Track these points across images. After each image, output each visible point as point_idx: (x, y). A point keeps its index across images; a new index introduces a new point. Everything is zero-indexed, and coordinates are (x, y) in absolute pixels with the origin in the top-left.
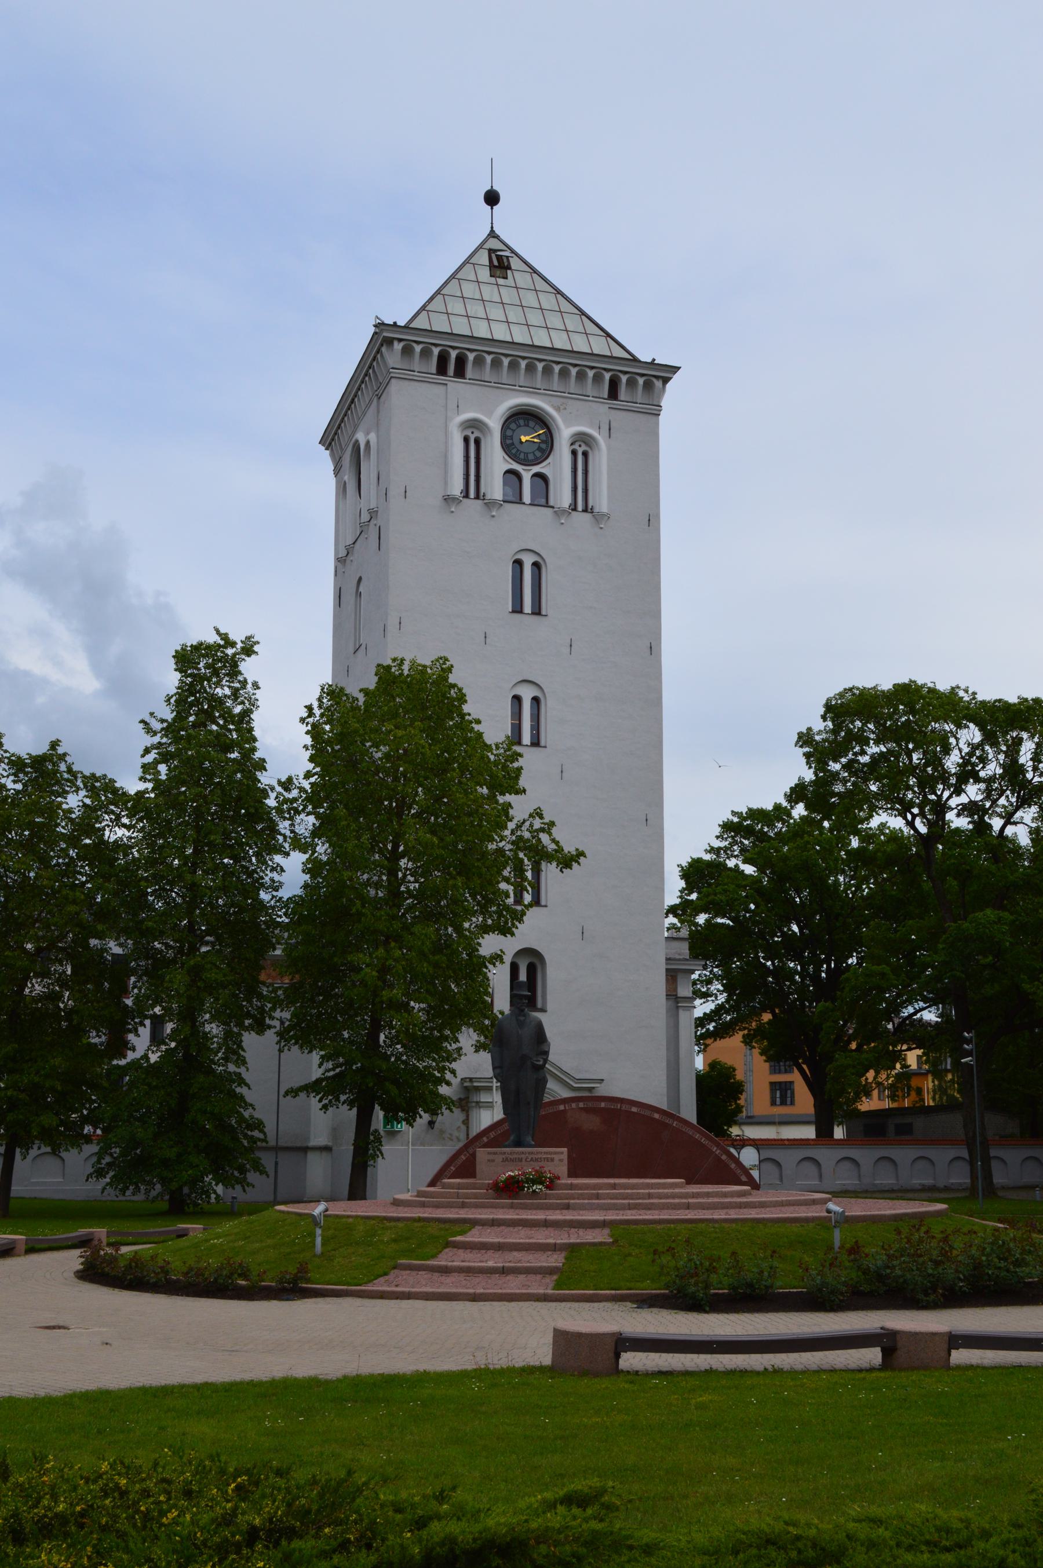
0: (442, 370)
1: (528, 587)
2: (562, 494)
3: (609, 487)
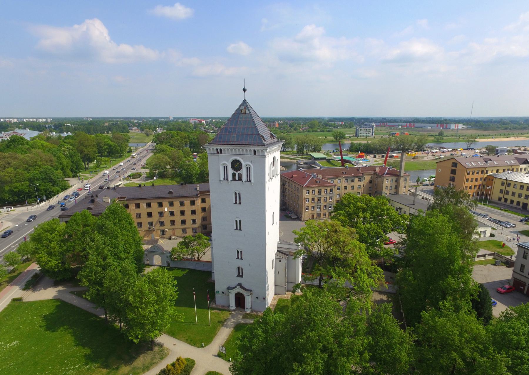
0: (218, 153)
1: (238, 199)
2: (244, 178)
3: (254, 177)
